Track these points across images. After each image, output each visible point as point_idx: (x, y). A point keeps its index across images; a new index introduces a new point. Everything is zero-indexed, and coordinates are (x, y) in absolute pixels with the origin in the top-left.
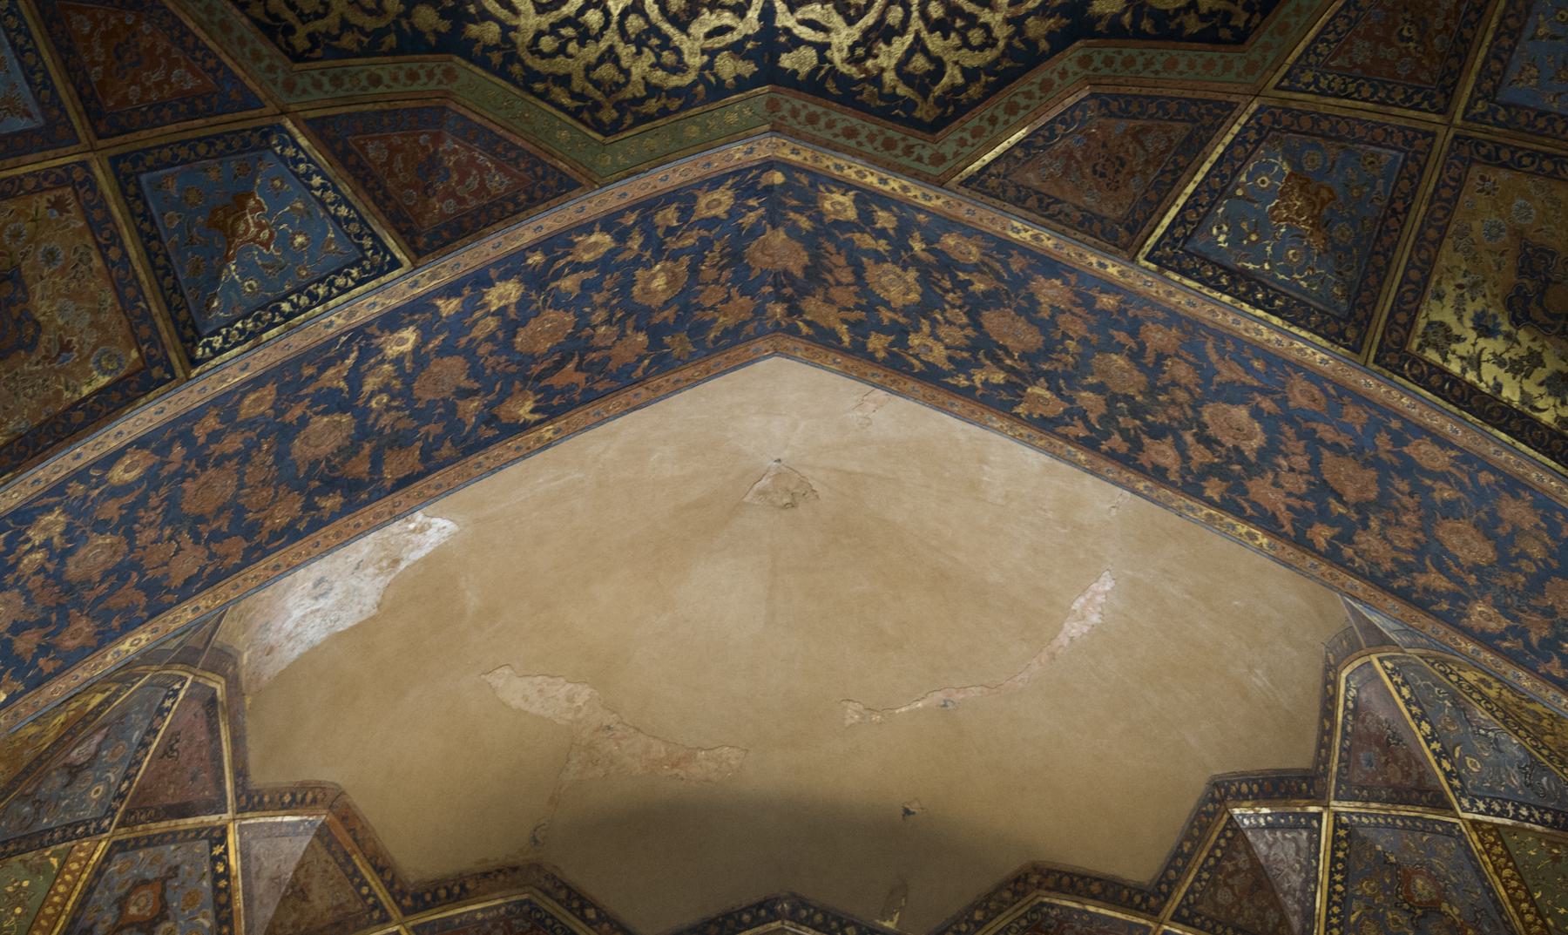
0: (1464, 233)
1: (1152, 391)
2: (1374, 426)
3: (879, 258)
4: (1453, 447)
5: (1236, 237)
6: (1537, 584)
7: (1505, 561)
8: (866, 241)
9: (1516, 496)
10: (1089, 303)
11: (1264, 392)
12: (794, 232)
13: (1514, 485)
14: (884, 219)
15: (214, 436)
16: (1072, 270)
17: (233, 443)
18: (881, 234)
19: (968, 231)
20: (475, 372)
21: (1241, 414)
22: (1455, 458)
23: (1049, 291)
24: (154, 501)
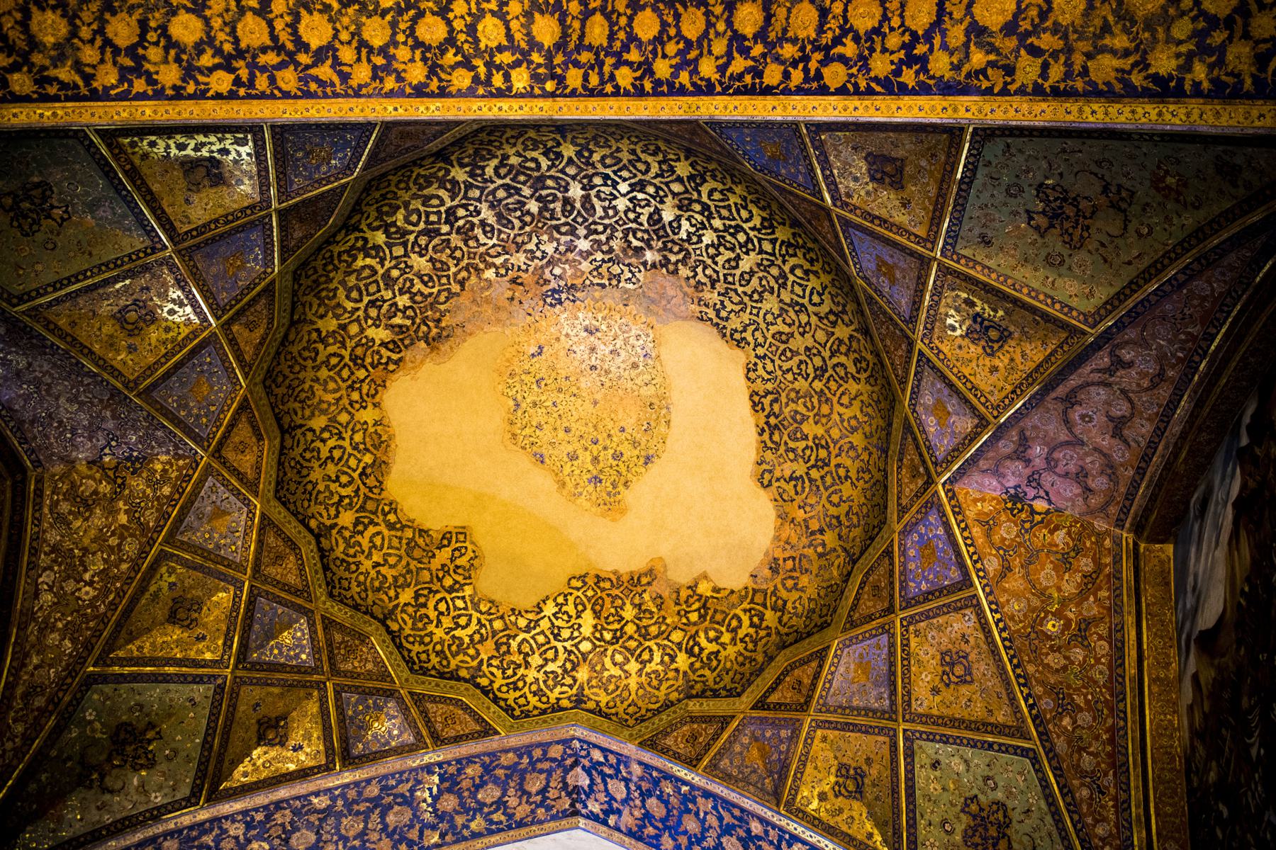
0: (251, 178)
1: (359, 26)
2: (251, 84)
3: (500, 49)
4: (212, 98)
5: (343, 138)
6: (143, 25)
7: (164, 30)
8: (506, 58)
9: (174, 87)
10: (399, 79)
11: (307, 67)
12: (540, 47)
13: (178, 94)
14: (498, 80)
15: (795, 64)
16: (409, 96)
17: (788, 51)
18: (499, 68)
19: (460, 94)
20: (677, 17)
21: (315, 44)
22: (208, 90)
23: (417, 73)
24: (830, 35)
